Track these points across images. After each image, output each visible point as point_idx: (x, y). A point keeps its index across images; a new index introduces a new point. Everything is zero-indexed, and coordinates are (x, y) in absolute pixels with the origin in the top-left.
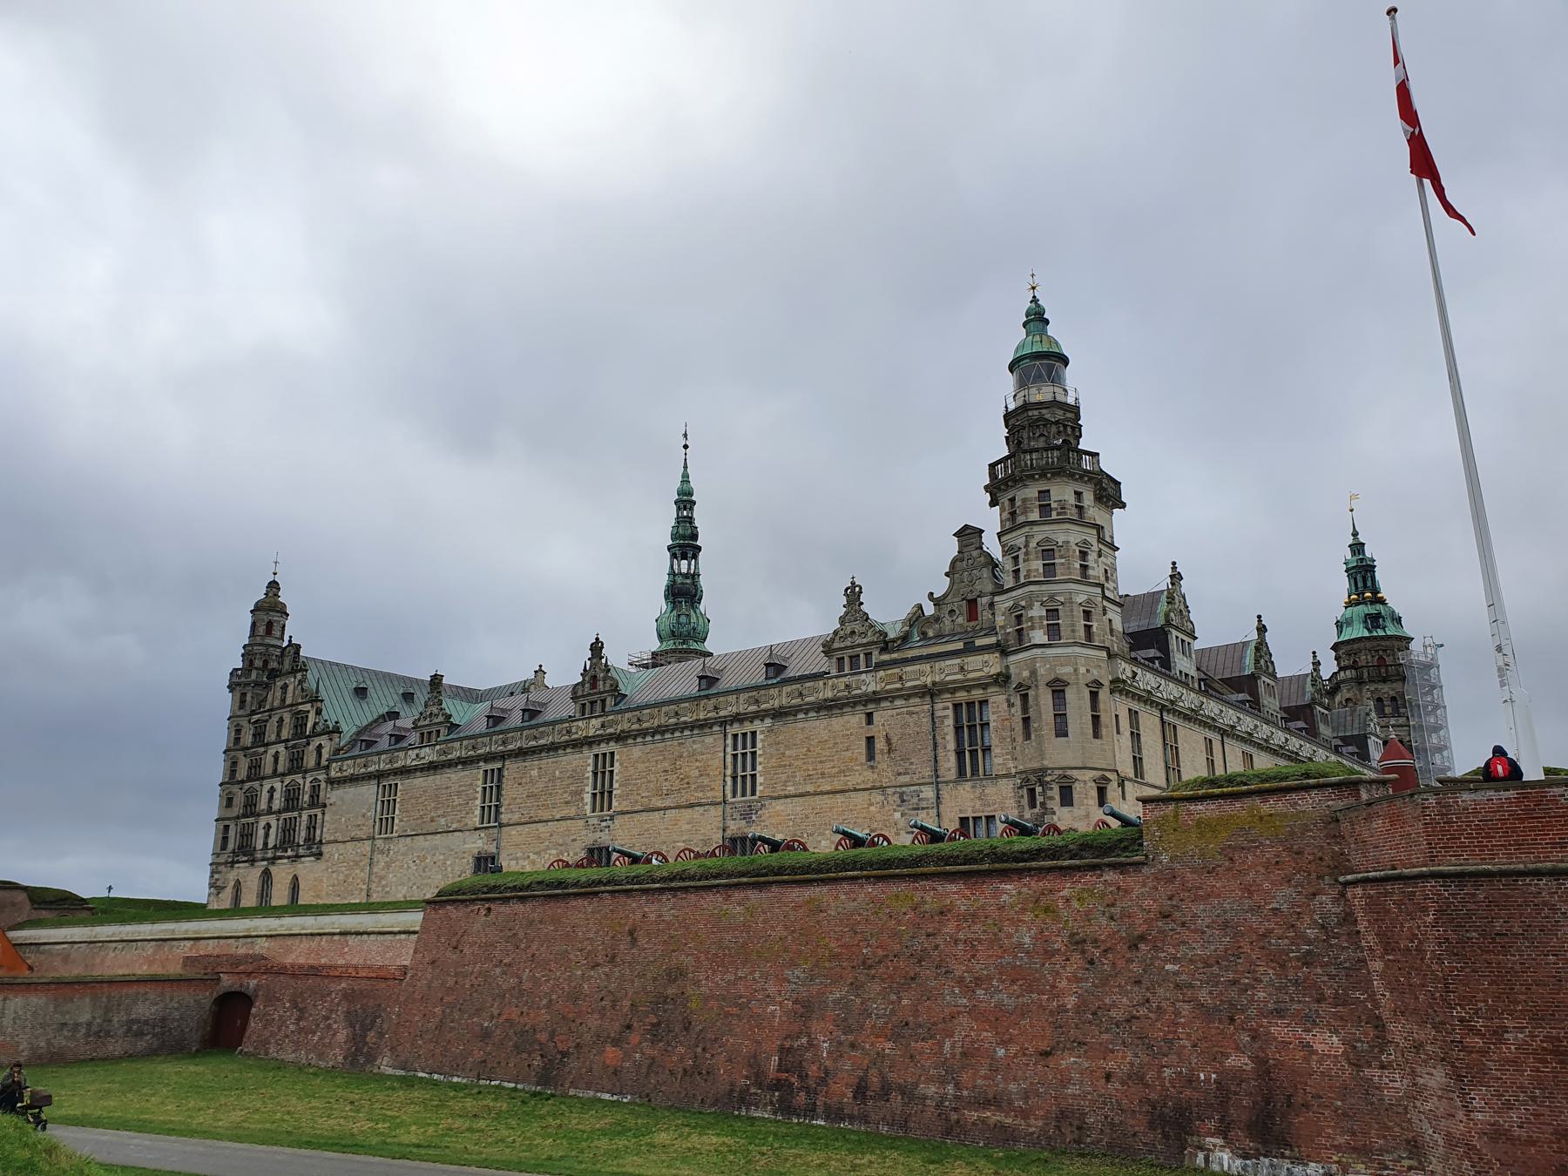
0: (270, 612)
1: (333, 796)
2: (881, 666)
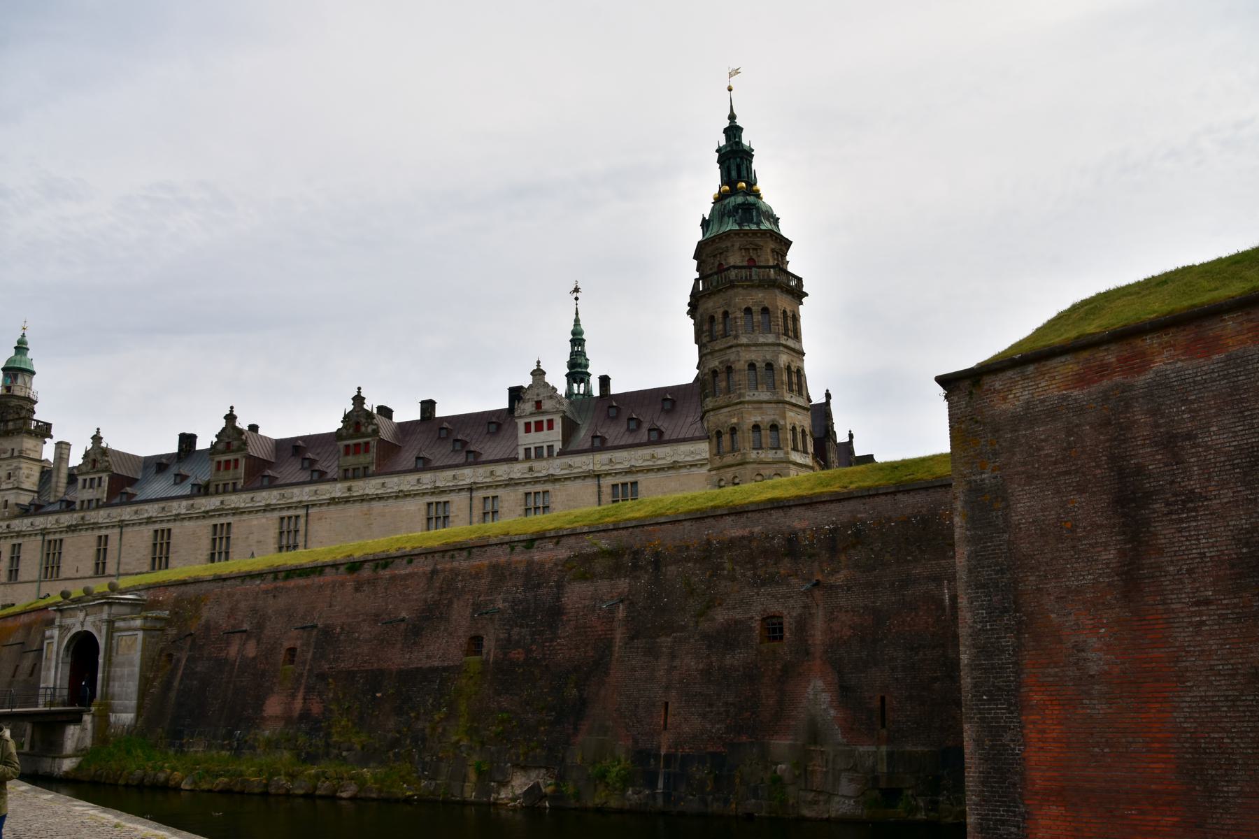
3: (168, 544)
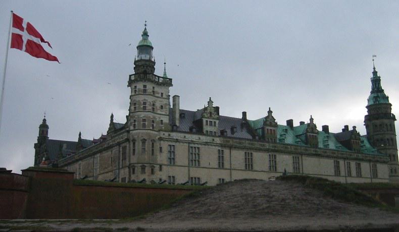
0: (44, 128)
3: (252, 159)
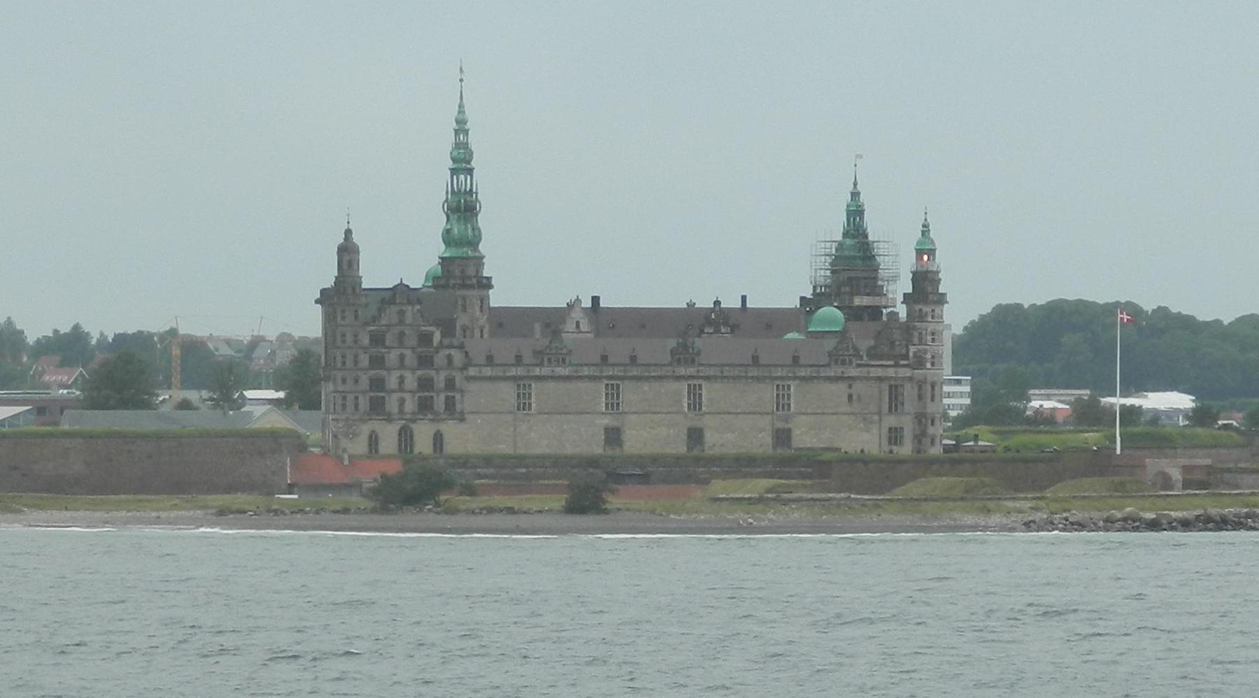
1: (473, 387)
2: (859, 366)
